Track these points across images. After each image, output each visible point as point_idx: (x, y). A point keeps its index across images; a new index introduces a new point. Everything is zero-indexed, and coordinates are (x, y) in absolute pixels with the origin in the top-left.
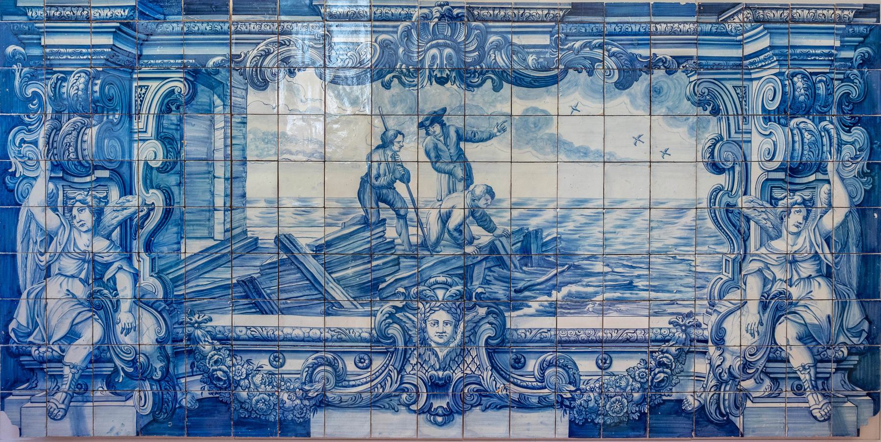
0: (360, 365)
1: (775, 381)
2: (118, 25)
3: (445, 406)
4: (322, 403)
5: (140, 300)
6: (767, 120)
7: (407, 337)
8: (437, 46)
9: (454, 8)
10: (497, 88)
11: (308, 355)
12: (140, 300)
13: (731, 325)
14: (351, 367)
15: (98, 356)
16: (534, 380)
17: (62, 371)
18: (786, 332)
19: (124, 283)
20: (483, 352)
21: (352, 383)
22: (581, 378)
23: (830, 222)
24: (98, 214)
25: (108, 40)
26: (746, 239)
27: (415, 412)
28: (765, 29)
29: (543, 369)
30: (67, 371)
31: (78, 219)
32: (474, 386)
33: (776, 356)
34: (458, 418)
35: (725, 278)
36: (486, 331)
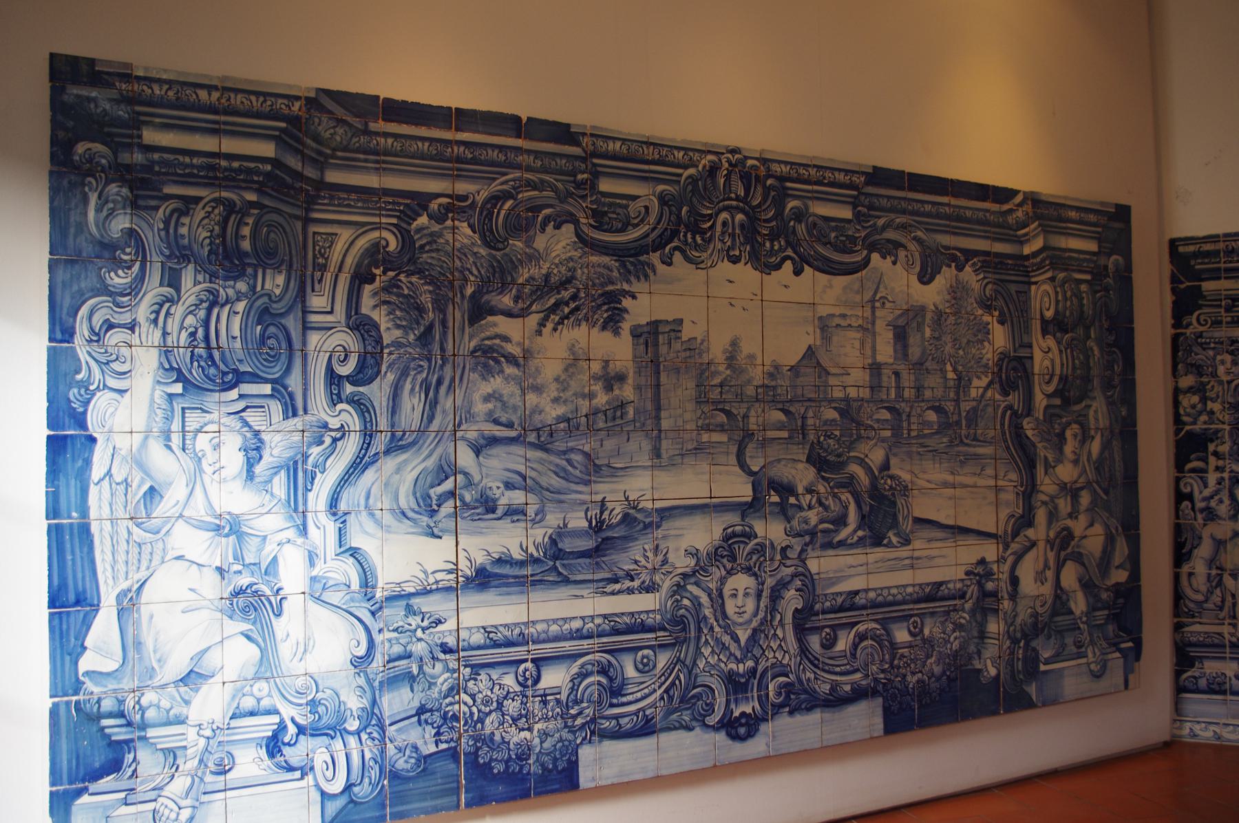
0: (647, 668)
2: (283, 125)
5: (317, 591)
6: (1045, 332)
8: (726, 208)
9: (746, 158)
10: (798, 272)
12: (317, 591)
13: (1027, 571)
14: (630, 672)
16: (846, 662)
18: (1070, 577)
20: (789, 629)
25: (267, 149)
28: (1040, 225)
32: (782, 679)
35: (1017, 515)
36: (792, 600)
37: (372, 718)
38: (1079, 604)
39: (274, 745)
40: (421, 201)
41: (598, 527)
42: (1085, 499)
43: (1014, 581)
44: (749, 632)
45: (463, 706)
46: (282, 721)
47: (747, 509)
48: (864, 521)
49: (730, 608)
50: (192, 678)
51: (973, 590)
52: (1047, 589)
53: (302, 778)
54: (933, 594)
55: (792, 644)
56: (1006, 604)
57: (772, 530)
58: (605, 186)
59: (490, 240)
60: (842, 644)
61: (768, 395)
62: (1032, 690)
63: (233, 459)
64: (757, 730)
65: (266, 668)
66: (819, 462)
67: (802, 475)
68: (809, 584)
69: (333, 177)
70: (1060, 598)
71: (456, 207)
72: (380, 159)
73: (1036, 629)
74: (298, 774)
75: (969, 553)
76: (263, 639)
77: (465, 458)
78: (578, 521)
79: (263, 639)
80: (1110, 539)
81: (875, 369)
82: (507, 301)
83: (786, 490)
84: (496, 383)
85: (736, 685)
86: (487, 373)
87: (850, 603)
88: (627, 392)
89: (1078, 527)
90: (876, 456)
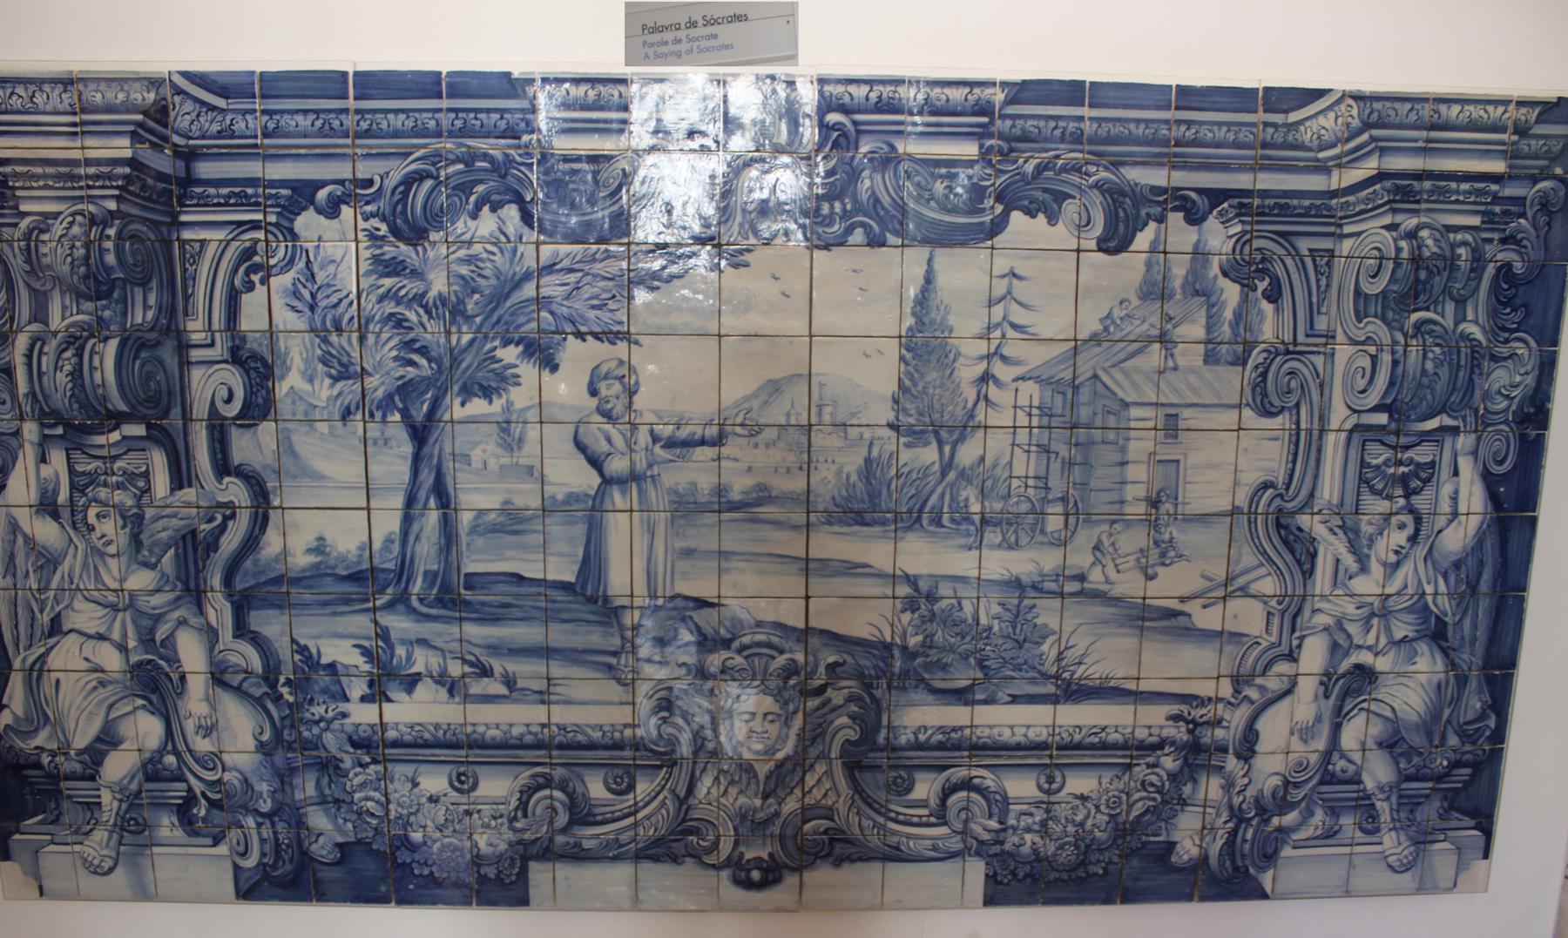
1: (1333, 811)
3: (766, 857)
4: (548, 853)
7: (699, 741)
11: (522, 768)
15: (152, 770)
17: (99, 797)
21: (599, 818)
22: (1011, 807)
23: (1455, 539)
24: (135, 522)
26: (1309, 574)
27: (713, 866)
29: (947, 793)
30: (106, 797)
31: (98, 533)
34: (791, 880)
39: (184, 812)
44: (771, 765)
46: (190, 790)
53: (215, 845)
64: (777, 880)
74: (209, 841)
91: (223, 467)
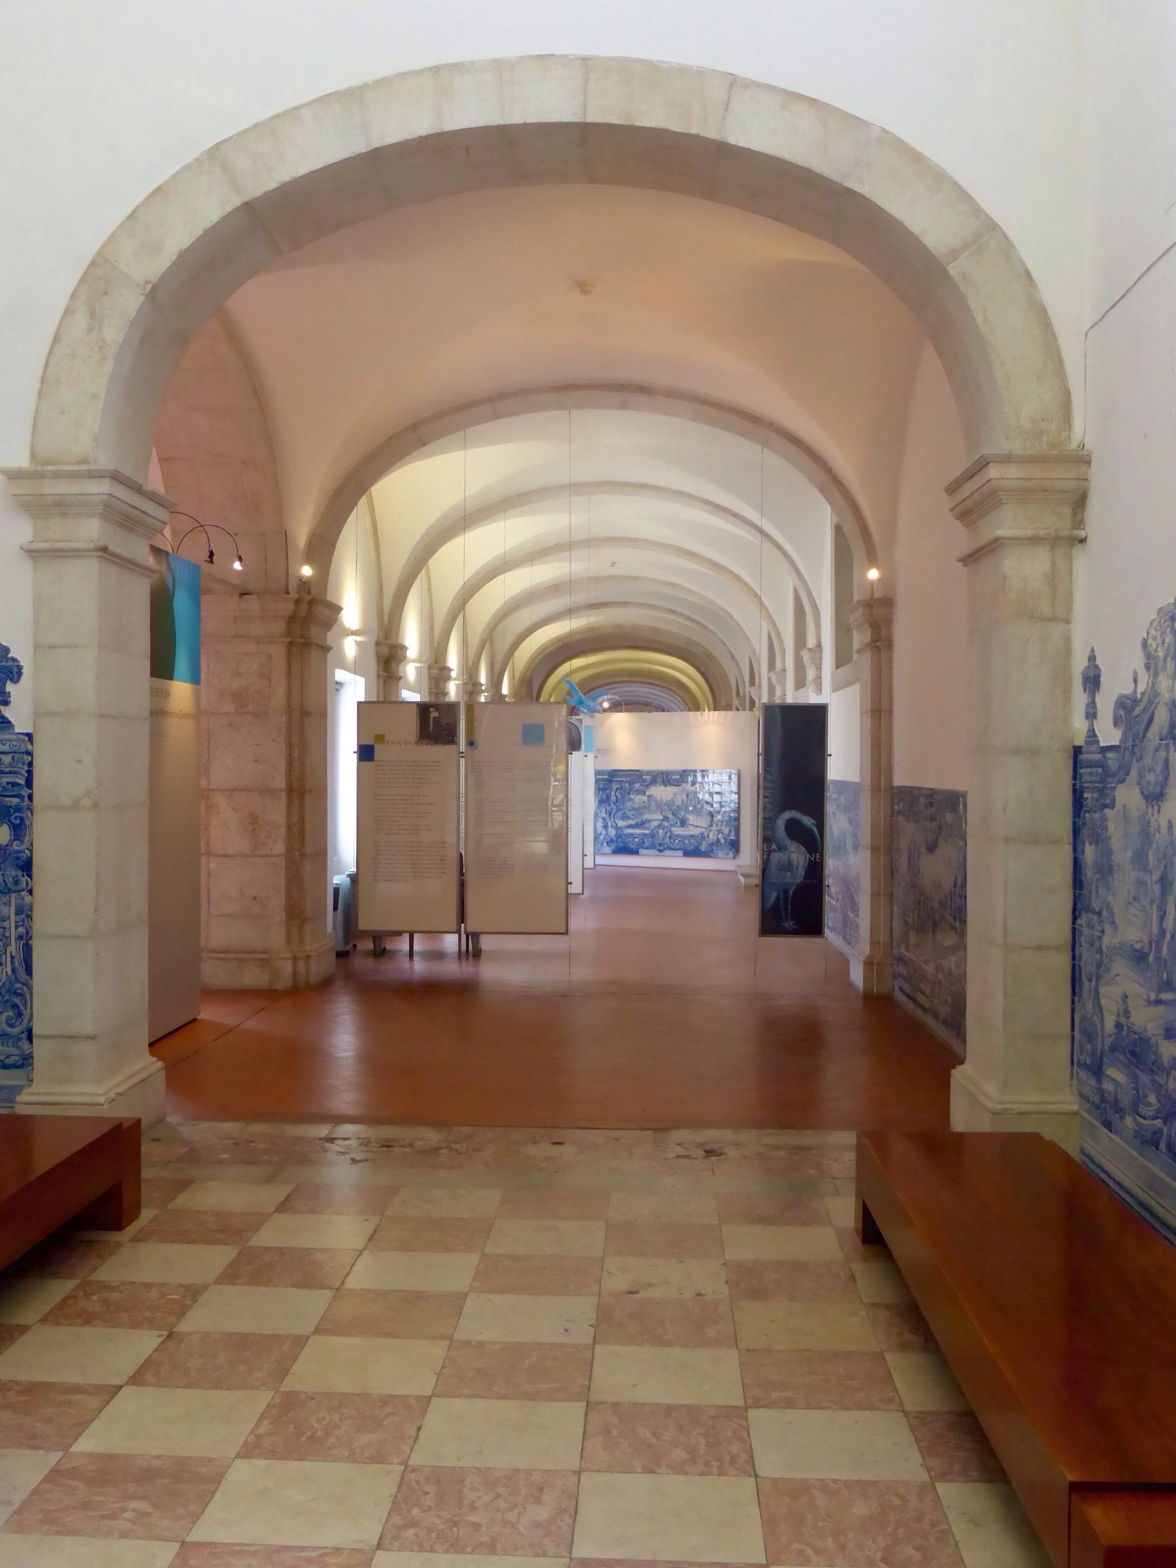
5: (612, 826)
18: (720, 836)
19: (609, 824)
25: (607, 777)
33: (718, 841)
36: (668, 834)
37: (617, 842)
38: (723, 841)
39: (607, 842)
40: (622, 781)
41: (642, 821)
42: (724, 823)
43: (708, 836)
45: (626, 841)
47: (662, 820)
48: (681, 824)
49: (660, 833)
50: (600, 834)
51: (700, 836)
52: (715, 838)
54: (693, 836)
55: (668, 839)
56: (706, 839)
57: (666, 824)
58: (644, 777)
59: (630, 785)
60: (677, 841)
61: (665, 804)
62: (712, 854)
63: (604, 811)
65: (607, 834)
66: (673, 814)
67: (671, 816)
68: (671, 832)
69: (614, 779)
70: (718, 841)
71: (626, 782)
72: (617, 777)
73: (712, 844)
75: (700, 830)
76: (606, 830)
77: (627, 812)
78: (640, 820)
79: (606, 830)
80: (730, 831)
81: (683, 801)
82: (632, 793)
83: (668, 818)
84: (630, 803)
85: (660, 845)
86: (630, 801)
87: (678, 835)
88: (646, 804)
89: (723, 828)
90: (683, 814)
91: (614, 804)
